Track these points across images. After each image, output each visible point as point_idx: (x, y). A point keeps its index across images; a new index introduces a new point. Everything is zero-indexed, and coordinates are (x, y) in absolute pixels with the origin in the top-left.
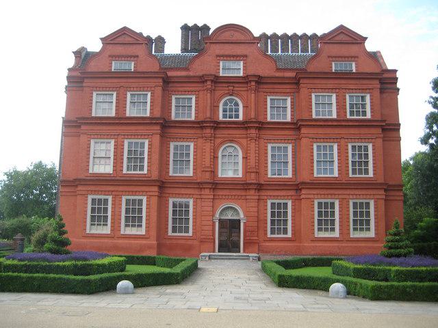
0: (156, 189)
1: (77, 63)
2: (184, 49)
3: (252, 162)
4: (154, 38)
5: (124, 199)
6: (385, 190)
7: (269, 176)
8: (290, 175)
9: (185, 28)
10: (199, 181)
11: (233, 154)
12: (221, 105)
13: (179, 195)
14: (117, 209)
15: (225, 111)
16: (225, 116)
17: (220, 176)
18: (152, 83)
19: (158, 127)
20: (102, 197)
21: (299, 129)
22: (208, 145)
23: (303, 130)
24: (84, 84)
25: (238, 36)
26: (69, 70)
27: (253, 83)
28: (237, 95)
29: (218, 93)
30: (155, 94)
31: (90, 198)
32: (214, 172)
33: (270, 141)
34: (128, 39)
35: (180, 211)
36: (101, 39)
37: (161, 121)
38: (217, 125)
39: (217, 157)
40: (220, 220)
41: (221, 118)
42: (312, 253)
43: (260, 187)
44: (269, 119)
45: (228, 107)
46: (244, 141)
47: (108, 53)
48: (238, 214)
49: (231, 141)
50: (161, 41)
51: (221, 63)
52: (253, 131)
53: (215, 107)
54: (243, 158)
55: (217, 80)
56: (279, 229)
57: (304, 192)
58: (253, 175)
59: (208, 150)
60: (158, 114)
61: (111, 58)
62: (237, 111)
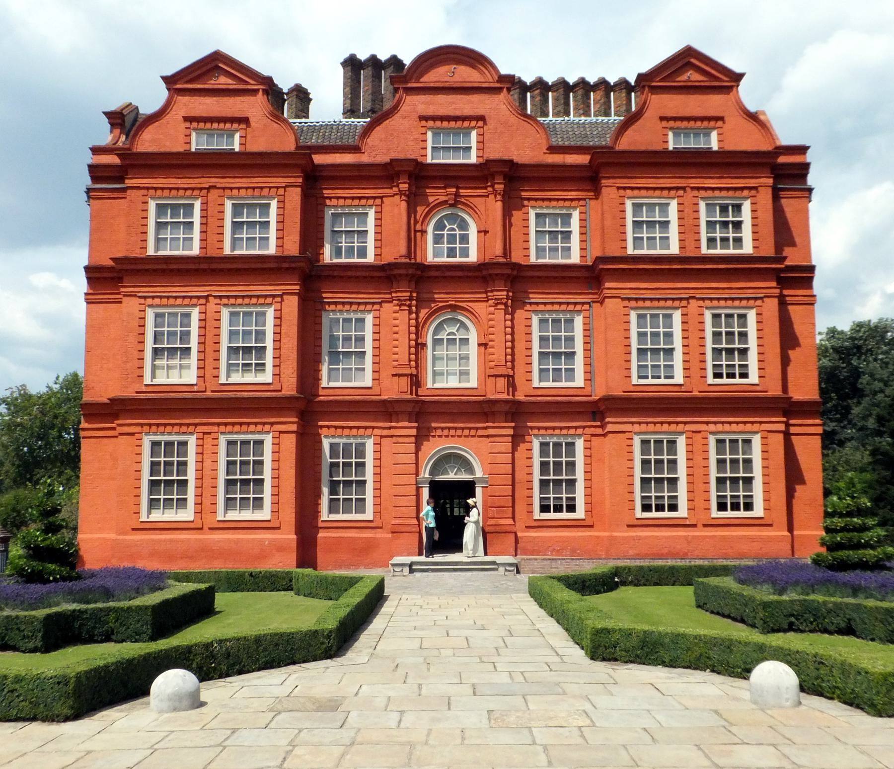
2: (351, 111)
3: (499, 353)
4: (285, 90)
8: (579, 381)
9: (352, 64)
11: (458, 337)
12: (430, 229)
14: (208, 464)
15: (438, 239)
17: (430, 385)
24: (129, 182)
26: (96, 150)
30: (287, 205)
34: (223, 81)
36: (165, 79)
37: (302, 264)
39: (424, 345)
41: (430, 258)
42: (631, 552)
45: (445, 232)
46: (481, 308)
47: (183, 113)
48: (470, 469)
49: (454, 308)
51: (430, 135)
53: (414, 235)
54: (479, 345)
58: (502, 383)
59: (403, 328)
60: (293, 248)
61: (188, 124)
62: (465, 239)
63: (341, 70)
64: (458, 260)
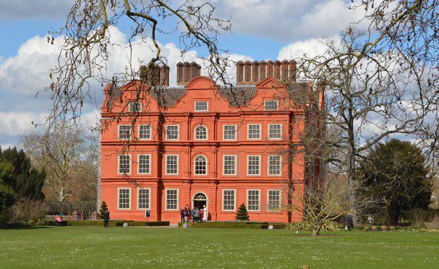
9: (180, 65)
10: (182, 178)
13: (170, 186)
15: (197, 133)
22: (186, 156)
28: (207, 125)
29: (193, 123)
32: (190, 173)
35: (172, 194)
38: (192, 145)
40: (195, 201)
41: (195, 139)
43: (217, 182)
44: (223, 140)
48: (205, 198)
55: (191, 116)
62: (205, 133)
64: (203, 140)
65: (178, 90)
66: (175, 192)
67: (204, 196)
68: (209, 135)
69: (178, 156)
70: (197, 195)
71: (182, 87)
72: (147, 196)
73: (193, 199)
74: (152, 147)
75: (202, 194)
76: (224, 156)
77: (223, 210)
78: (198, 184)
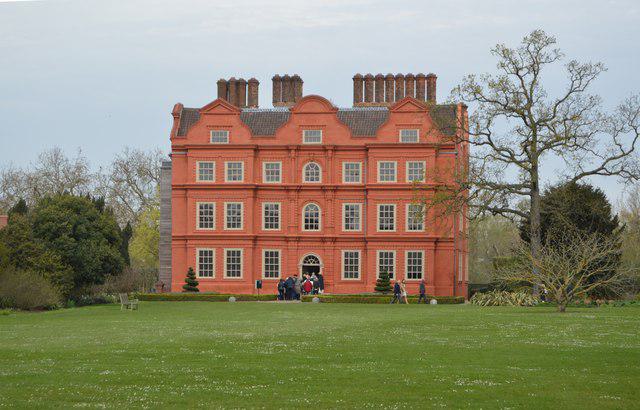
0: (251, 242)
1: (176, 124)
5: (225, 250)
6: (435, 243)
7: (344, 230)
9: (276, 80)
10: (285, 235)
13: (268, 246)
16: (307, 179)
18: (243, 153)
19: (251, 192)
20: (208, 249)
21: (367, 190)
23: (370, 193)
25: (318, 108)
27: (330, 152)
28: (318, 161)
29: (301, 160)
31: (198, 250)
32: (298, 227)
33: (345, 201)
35: (272, 258)
38: (300, 189)
41: (304, 182)
43: (334, 240)
44: (344, 182)
49: (310, 201)
50: (254, 83)
52: (330, 193)
55: (299, 149)
56: (351, 274)
57: (369, 243)
62: (317, 174)
63: (272, 82)
64: (315, 182)
65: (276, 113)
66: (277, 254)
67: (316, 259)
68: (324, 180)
69: (395, 206)
70: (306, 259)
71: (285, 109)
72: (277, 261)
73: (301, 263)
74: (245, 192)
75: (313, 257)
76: (344, 205)
77: (343, 279)
78: (309, 244)
